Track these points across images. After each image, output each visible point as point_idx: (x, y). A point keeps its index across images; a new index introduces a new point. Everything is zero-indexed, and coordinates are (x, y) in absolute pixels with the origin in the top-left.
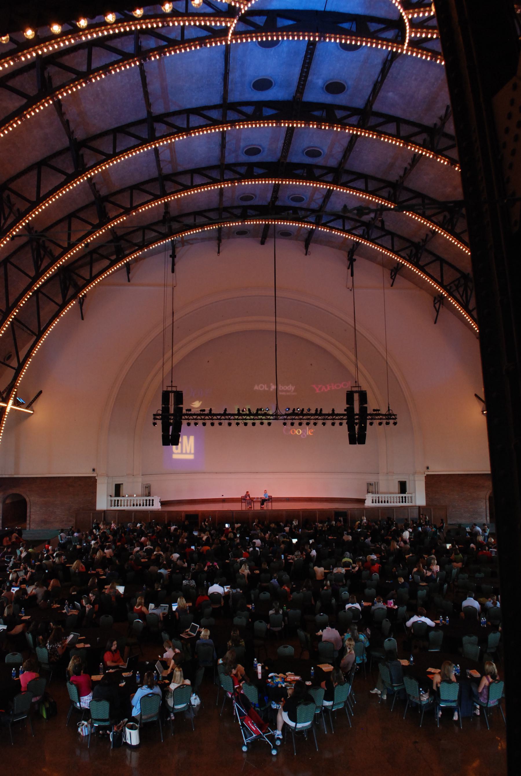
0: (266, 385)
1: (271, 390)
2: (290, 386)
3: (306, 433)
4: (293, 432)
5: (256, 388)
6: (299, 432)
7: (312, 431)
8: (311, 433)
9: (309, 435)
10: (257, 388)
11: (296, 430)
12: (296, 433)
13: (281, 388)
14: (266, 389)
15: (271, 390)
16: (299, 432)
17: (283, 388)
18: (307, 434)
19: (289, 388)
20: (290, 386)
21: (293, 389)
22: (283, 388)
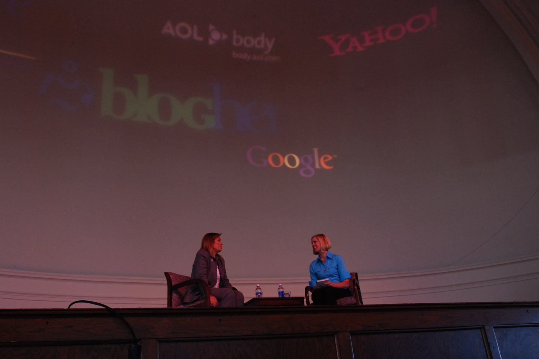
0: (195, 28)
1: (211, 42)
2: (262, 38)
3: (313, 165)
4: (276, 160)
5: (168, 29)
6: (292, 161)
7: (330, 158)
8: (327, 164)
9: (322, 169)
10: (171, 31)
11: (284, 157)
12: (284, 164)
13: (238, 41)
14: (196, 38)
15: (211, 42)
16: (292, 161)
17: (243, 41)
18: (317, 166)
19: (259, 43)
20: (262, 38)
21: (270, 46)
22: (243, 41)
